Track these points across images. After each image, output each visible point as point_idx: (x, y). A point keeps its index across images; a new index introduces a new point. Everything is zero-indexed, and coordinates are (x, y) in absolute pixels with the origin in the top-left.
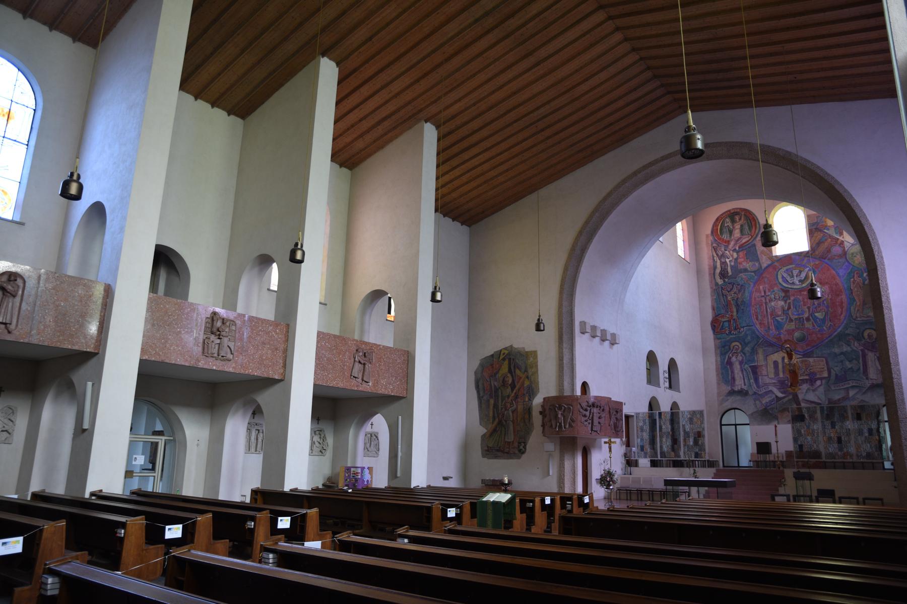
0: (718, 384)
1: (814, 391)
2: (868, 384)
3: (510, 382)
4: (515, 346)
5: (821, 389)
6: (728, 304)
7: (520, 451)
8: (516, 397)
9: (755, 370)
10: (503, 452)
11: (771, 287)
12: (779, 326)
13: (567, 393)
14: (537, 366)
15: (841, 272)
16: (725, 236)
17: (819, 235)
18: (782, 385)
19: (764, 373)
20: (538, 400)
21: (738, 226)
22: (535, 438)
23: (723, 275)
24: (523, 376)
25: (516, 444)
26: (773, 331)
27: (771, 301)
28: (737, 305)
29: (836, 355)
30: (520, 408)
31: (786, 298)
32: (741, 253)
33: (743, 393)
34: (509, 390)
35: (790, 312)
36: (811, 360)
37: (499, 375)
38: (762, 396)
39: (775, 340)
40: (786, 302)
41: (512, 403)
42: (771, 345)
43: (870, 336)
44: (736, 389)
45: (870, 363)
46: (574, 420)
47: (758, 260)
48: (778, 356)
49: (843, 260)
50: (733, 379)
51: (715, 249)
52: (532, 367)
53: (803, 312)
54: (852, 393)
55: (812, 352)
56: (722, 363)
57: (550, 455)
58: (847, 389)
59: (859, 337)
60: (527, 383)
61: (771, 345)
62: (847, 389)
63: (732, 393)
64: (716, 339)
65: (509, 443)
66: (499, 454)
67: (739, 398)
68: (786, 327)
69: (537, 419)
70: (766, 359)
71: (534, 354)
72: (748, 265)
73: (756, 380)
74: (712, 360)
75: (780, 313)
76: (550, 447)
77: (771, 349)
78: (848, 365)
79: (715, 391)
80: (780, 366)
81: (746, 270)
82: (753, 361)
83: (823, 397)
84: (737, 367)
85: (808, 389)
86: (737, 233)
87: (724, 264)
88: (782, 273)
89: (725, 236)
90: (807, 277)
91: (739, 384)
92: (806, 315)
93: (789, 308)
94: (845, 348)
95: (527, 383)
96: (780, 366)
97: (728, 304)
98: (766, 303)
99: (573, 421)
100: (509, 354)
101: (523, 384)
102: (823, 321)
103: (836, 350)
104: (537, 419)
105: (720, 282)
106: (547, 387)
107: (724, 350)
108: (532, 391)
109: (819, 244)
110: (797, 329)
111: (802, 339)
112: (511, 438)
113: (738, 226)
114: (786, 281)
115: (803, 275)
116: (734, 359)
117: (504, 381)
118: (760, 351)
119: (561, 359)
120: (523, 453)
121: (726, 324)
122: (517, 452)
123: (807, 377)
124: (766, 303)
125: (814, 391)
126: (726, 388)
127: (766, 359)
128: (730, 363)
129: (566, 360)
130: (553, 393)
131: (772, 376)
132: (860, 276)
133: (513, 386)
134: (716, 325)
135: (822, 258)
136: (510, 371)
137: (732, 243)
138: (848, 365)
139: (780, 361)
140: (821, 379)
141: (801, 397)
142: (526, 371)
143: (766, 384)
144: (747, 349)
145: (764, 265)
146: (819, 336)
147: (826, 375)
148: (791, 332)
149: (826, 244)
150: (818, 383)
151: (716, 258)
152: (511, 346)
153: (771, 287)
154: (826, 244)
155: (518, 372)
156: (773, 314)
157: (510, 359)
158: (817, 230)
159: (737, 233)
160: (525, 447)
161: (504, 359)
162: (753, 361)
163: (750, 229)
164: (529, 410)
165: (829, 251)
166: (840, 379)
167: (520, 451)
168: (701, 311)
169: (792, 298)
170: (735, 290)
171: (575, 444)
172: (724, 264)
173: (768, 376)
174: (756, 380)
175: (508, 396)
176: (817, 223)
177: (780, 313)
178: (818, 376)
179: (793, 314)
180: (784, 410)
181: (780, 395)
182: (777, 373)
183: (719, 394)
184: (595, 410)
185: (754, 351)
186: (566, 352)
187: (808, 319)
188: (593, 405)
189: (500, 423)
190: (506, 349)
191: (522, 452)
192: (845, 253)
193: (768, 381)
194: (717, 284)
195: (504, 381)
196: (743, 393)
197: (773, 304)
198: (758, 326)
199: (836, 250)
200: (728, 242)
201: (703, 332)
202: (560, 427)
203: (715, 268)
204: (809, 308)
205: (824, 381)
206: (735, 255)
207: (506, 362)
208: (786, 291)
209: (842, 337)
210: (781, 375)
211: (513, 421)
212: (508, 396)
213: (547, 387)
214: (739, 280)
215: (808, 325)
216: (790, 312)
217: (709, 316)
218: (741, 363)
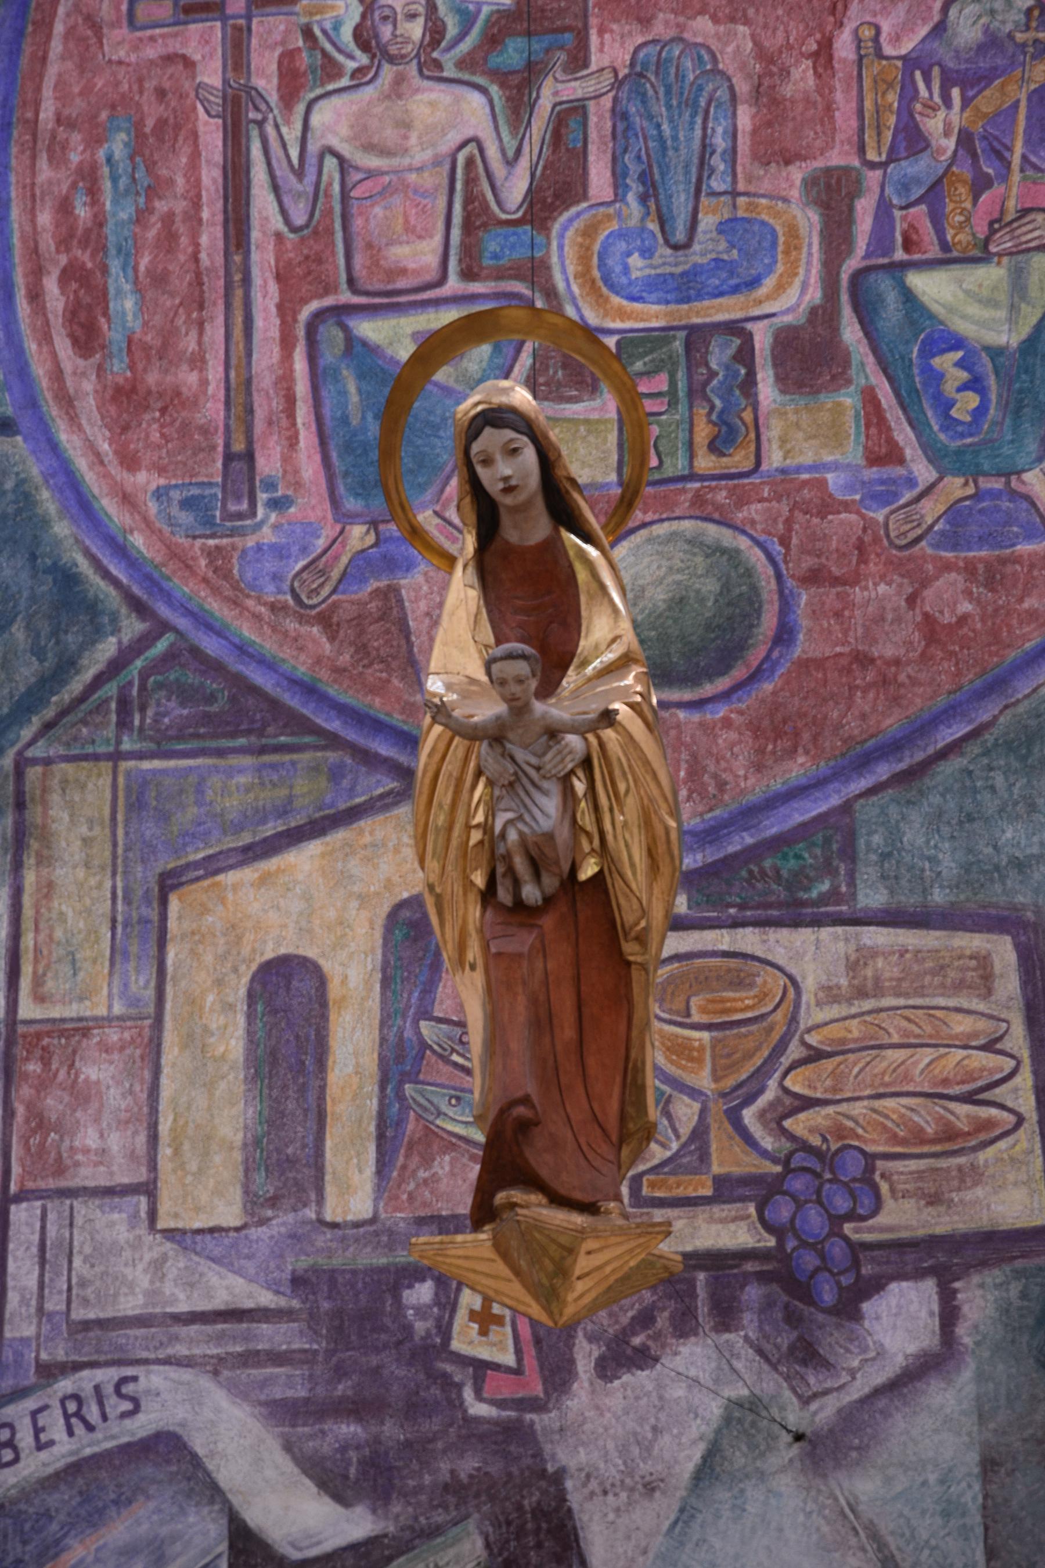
1: (822, 1451)
19: (102, 1145)
27: (308, 73)
35: (563, 251)
36: (810, 955)
39: (305, 652)
40: (518, 91)
42: (242, 713)
53: (750, 252)
55: (838, 834)
61: (242, 713)
70: (144, 929)
75: (420, 255)
77: (235, 784)
80: (353, 1046)
85: (745, 1417)
92: (788, 297)
93: (557, 190)
96: (353, 1046)
98: (237, 112)
118: (78, 811)
123: (732, 1231)
124: (237, 112)
125: (822, 1451)
127: (144, 929)
139: (354, 974)
140: (940, 1260)
143: (100, 1339)
146: (951, 597)
150: (900, 1320)
169: (611, 49)
177: (420, 255)
178: (899, 1216)
179: (603, 281)
182: (284, 1163)
187: (808, 358)
193: (132, 1273)
197: (333, 119)
198: (84, 440)
204: (833, 194)
205: (980, 1299)
210: (352, 1190)
215: (803, 438)
216: (563, 251)
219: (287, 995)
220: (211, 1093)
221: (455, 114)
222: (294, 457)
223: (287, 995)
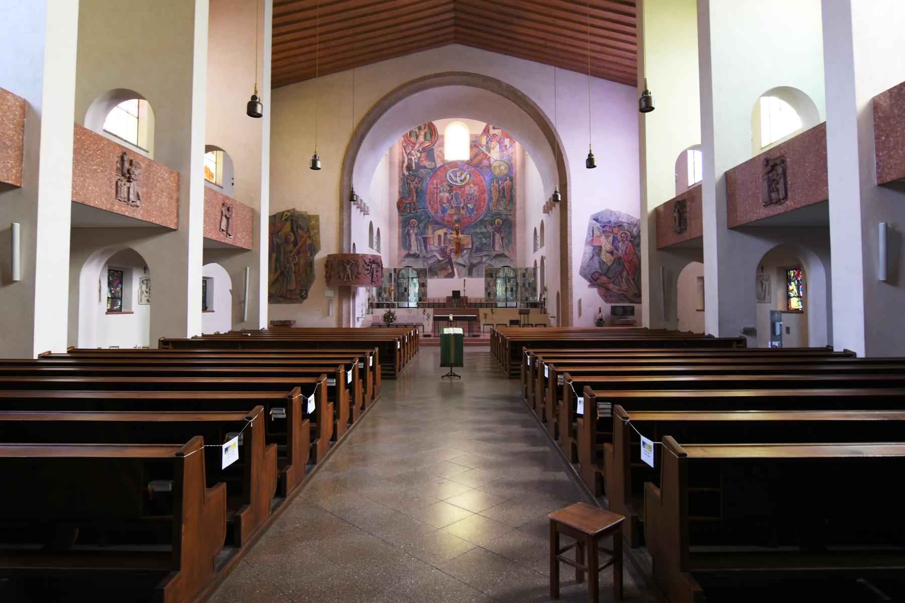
0: (399, 248)
2: (494, 253)
3: (293, 239)
4: (298, 209)
5: (467, 256)
6: (410, 190)
7: (302, 297)
8: (298, 252)
9: (425, 240)
10: (285, 298)
11: (442, 182)
12: (444, 211)
13: (346, 252)
14: (318, 228)
15: (487, 178)
16: (413, 139)
17: (476, 150)
18: (443, 252)
20: (320, 256)
21: (422, 133)
22: (318, 286)
23: (409, 168)
24: (305, 236)
25: (298, 292)
26: (440, 214)
28: (417, 192)
29: (477, 234)
30: (302, 262)
31: (450, 191)
32: (423, 154)
33: (416, 256)
34: (291, 246)
37: (282, 233)
38: (429, 259)
41: (294, 258)
42: (437, 223)
43: (498, 223)
44: (412, 253)
45: (496, 241)
46: (346, 271)
47: (434, 161)
48: (441, 232)
49: (488, 170)
50: (410, 245)
51: (405, 148)
52: (314, 229)
54: (484, 259)
56: (403, 234)
57: (330, 300)
58: (482, 257)
59: (492, 223)
60: (309, 242)
61: (437, 223)
62: (482, 257)
63: (408, 255)
64: (400, 215)
65: (291, 291)
66: (281, 299)
67: (413, 259)
68: (449, 212)
69: (319, 271)
70: (433, 233)
71: (317, 218)
72: (427, 164)
73: (426, 247)
74: (396, 231)
76: (330, 293)
77: (437, 226)
78: (484, 241)
79: (396, 253)
81: (425, 167)
82: (425, 234)
83: (467, 261)
84: (413, 237)
86: (421, 139)
87: (410, 160)
88: (449, 173)
89: (413, 139)
90: (465, 178)
91: (414, 249)
94: (484, 230)
95: (309, 242)
97: (410, 190)
99: (359, 273)
100: (291, 216)
101: (305, 242)
102: (472, 210)
103: (478, 231)
104: (319, 271)
105: (406, 173)
106: (328, 246)
107: (405, 224)
108: (314, 248)
109: (475, 156)
110: (456, 214)
111: (458, 221)
112: (293, 286)
113: (422, 133)
114: (452, 179)
115: (463, 177)
116: (411, 231)
117: (286, 238)
118: (430, 227)
119: (341, 224)
120: (305, 298)
121: (408, 205)
122: (298, 297)
126: (405, 252)
127: (433, 233)
128: (408, 234)
129: (345, 225)
130: (333, 251)
131: (436, 245)
132: (497, 182)
133: (295, 243)
134: (401, 205)
135: (476, 166)
136: (292, 230)
137: (417, 145)
138: (484, 241)
141: (453, 260)
142: (308, 231)
144: (422, 225)
145: (438, 166)
147: (470, 246)
148: (451, 216)
149: (479, 158)
150: (465, 251)
151: (405, 155)
152: (294, 209)
153: (442, 182)
154: (479, 158)
155: (300, 232)
156: (441, 202)
157: (292, 221)
158: (476, 146)
159: (421, 139)
160: (306, 294)
161: (286, 220)
162: (425, 234)
163: (431, 136)
164: (311, 264)
165: (481, 162)
166: (479, 250)
167: (302, 297)
168: (390, 194)
170: (416, 180)
171: (347, 292)
172: (410, 160)
173: (434, 245)
174: (426, 247)
175: (291, 252)
176: (475, 141)
180: (442, 269)
181: (441, 259)
182: (439, 244)
183: (399, 256)
184: (374, 266)
185: (426, 227)
186: (345, 218)
187: (463, 208)
188: (374, 262)
189: (282, 273)
190: (288, 211)
191: (304, 298)
192: (490, 166)
193: (433, 248)
194: (404, 175)
195: (286, 238)
196: (416, 256)
199: (485, 162)
200: (415, 144)
201: (390, 209)
202: (348, 278)
203: (403, 162)
206: (419, 155)
207: (289, 223)
208: (451, 186)
209: (482, 222)
211: (295, 273)
212: (291, 252)
213: (328, 246)
214: (420, 173)
215: (463, 212)
217: (396, 198)
218: (416, 234)
219: (440, 236)
220: (436, 241)
221: (447, 194)
222: (440, 211)
223: (440, 236)
